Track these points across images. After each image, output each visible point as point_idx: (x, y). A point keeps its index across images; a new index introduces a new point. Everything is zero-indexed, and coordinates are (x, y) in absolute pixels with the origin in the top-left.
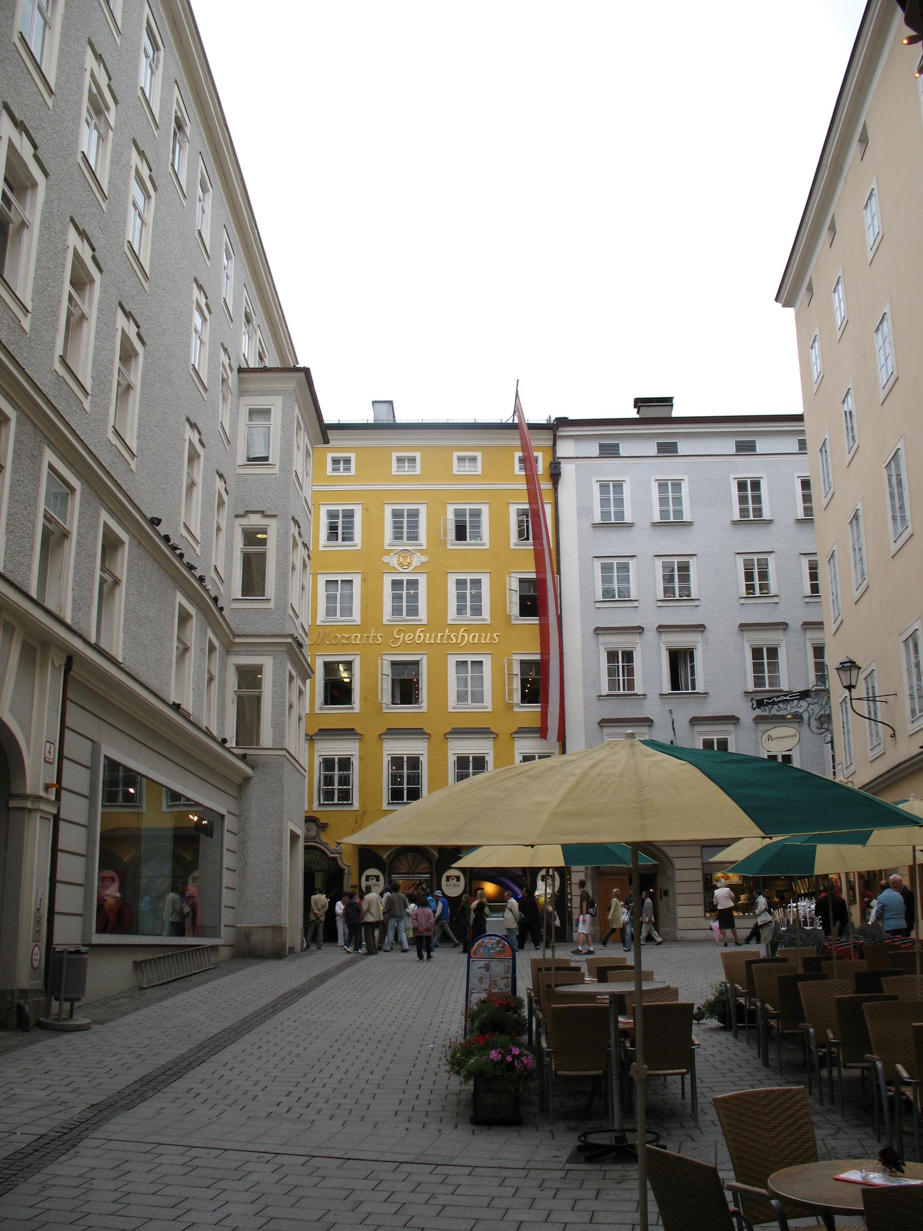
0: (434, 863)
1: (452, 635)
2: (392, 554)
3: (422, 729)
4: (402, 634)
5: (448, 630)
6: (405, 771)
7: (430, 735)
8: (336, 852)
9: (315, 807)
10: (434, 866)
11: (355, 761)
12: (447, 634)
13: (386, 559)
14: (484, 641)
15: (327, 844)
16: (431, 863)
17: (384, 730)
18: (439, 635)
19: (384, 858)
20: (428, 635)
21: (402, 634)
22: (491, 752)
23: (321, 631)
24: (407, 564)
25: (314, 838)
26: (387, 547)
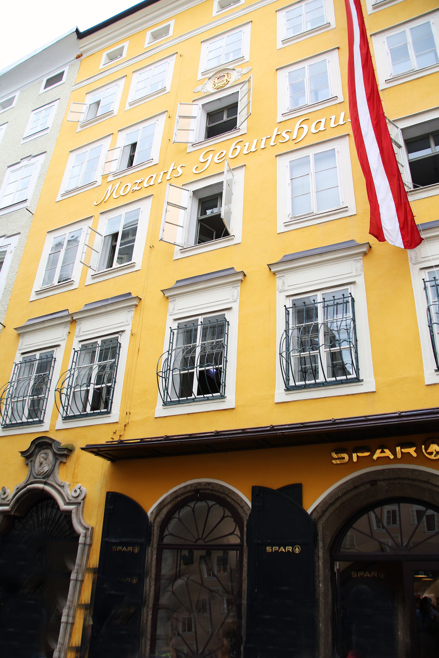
0: (245, 523)
1: (284, 134)
2: (205, 82)
3: (233, 268)
4: (211, 155)
5: (276, 130)
6: (199, 342)
7: (245, 275)
8: (74, 500)
9: (60, 424)
10: (245, 529)
11: (124, 340)
12: (275, 134)
13: (199, 88)
14: (334, 124)
15: (63, 487)
16: (238, 520)
17: (172, 284)
18: (264, 139)
19: (149, 513)
20: (247, 145)
21: (211, 155)
22: (360, 280)
23: (110, 188)
24: (224, 83)
25: (48, 475)
26: (200, 77)
